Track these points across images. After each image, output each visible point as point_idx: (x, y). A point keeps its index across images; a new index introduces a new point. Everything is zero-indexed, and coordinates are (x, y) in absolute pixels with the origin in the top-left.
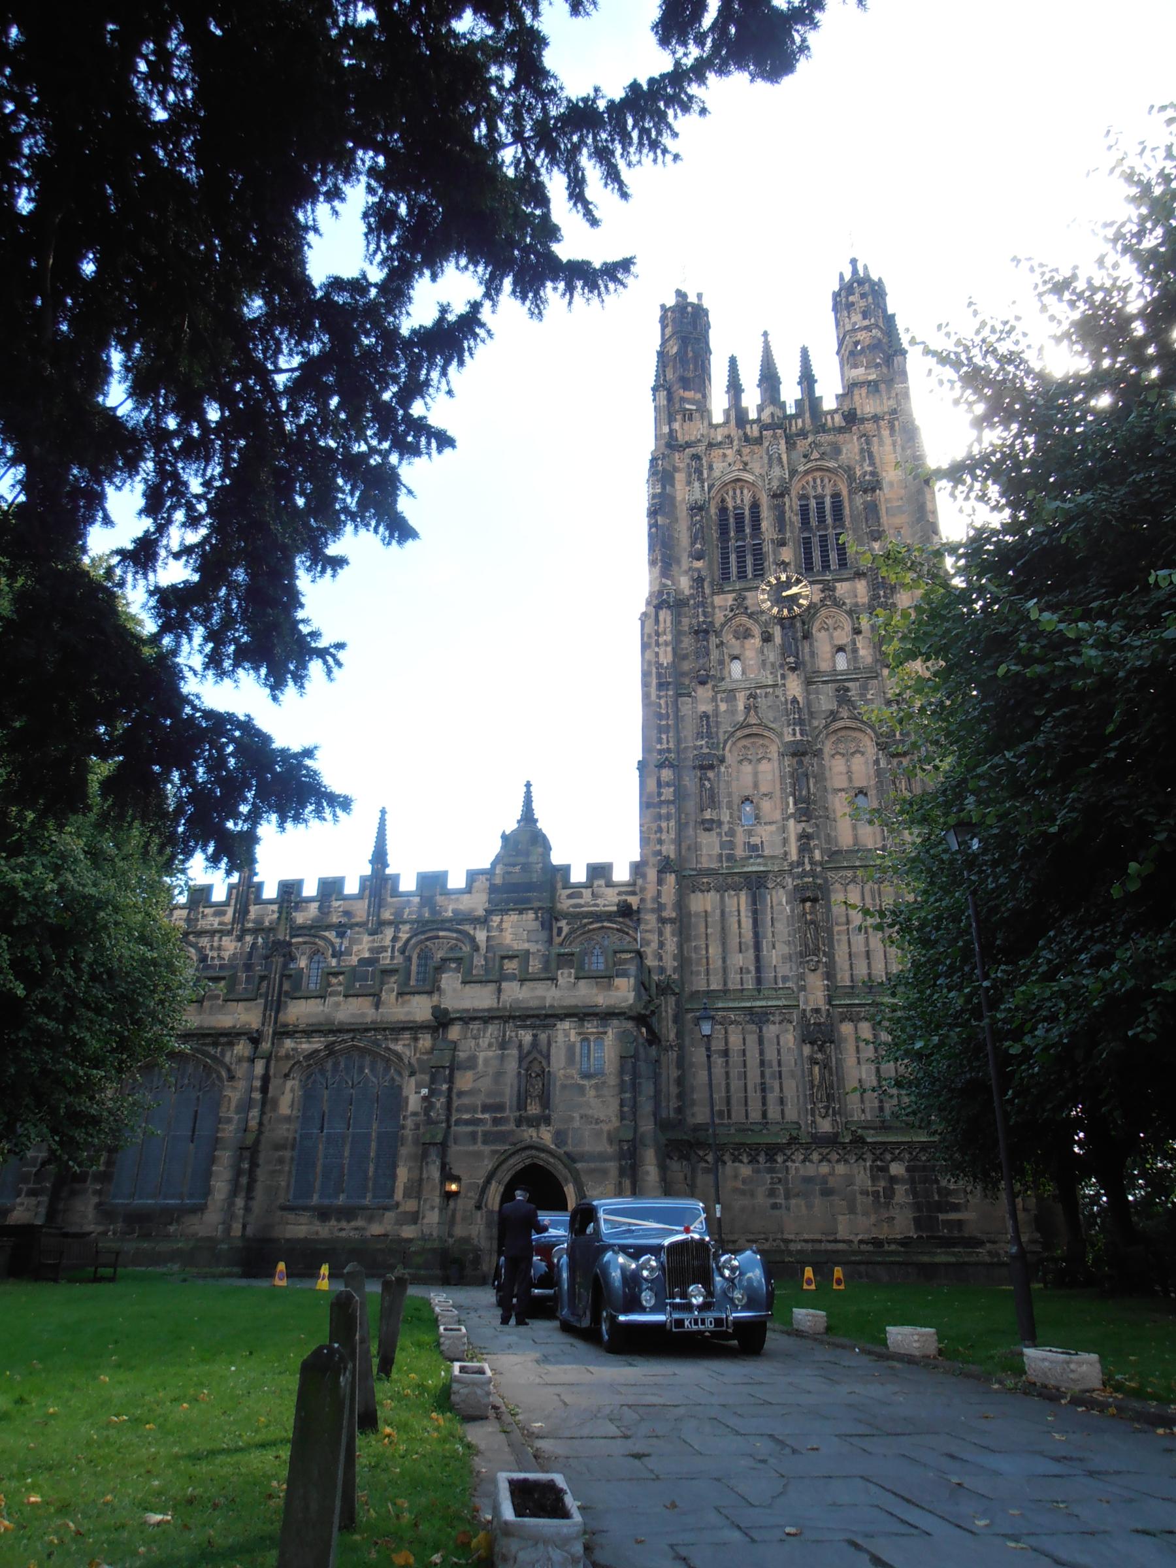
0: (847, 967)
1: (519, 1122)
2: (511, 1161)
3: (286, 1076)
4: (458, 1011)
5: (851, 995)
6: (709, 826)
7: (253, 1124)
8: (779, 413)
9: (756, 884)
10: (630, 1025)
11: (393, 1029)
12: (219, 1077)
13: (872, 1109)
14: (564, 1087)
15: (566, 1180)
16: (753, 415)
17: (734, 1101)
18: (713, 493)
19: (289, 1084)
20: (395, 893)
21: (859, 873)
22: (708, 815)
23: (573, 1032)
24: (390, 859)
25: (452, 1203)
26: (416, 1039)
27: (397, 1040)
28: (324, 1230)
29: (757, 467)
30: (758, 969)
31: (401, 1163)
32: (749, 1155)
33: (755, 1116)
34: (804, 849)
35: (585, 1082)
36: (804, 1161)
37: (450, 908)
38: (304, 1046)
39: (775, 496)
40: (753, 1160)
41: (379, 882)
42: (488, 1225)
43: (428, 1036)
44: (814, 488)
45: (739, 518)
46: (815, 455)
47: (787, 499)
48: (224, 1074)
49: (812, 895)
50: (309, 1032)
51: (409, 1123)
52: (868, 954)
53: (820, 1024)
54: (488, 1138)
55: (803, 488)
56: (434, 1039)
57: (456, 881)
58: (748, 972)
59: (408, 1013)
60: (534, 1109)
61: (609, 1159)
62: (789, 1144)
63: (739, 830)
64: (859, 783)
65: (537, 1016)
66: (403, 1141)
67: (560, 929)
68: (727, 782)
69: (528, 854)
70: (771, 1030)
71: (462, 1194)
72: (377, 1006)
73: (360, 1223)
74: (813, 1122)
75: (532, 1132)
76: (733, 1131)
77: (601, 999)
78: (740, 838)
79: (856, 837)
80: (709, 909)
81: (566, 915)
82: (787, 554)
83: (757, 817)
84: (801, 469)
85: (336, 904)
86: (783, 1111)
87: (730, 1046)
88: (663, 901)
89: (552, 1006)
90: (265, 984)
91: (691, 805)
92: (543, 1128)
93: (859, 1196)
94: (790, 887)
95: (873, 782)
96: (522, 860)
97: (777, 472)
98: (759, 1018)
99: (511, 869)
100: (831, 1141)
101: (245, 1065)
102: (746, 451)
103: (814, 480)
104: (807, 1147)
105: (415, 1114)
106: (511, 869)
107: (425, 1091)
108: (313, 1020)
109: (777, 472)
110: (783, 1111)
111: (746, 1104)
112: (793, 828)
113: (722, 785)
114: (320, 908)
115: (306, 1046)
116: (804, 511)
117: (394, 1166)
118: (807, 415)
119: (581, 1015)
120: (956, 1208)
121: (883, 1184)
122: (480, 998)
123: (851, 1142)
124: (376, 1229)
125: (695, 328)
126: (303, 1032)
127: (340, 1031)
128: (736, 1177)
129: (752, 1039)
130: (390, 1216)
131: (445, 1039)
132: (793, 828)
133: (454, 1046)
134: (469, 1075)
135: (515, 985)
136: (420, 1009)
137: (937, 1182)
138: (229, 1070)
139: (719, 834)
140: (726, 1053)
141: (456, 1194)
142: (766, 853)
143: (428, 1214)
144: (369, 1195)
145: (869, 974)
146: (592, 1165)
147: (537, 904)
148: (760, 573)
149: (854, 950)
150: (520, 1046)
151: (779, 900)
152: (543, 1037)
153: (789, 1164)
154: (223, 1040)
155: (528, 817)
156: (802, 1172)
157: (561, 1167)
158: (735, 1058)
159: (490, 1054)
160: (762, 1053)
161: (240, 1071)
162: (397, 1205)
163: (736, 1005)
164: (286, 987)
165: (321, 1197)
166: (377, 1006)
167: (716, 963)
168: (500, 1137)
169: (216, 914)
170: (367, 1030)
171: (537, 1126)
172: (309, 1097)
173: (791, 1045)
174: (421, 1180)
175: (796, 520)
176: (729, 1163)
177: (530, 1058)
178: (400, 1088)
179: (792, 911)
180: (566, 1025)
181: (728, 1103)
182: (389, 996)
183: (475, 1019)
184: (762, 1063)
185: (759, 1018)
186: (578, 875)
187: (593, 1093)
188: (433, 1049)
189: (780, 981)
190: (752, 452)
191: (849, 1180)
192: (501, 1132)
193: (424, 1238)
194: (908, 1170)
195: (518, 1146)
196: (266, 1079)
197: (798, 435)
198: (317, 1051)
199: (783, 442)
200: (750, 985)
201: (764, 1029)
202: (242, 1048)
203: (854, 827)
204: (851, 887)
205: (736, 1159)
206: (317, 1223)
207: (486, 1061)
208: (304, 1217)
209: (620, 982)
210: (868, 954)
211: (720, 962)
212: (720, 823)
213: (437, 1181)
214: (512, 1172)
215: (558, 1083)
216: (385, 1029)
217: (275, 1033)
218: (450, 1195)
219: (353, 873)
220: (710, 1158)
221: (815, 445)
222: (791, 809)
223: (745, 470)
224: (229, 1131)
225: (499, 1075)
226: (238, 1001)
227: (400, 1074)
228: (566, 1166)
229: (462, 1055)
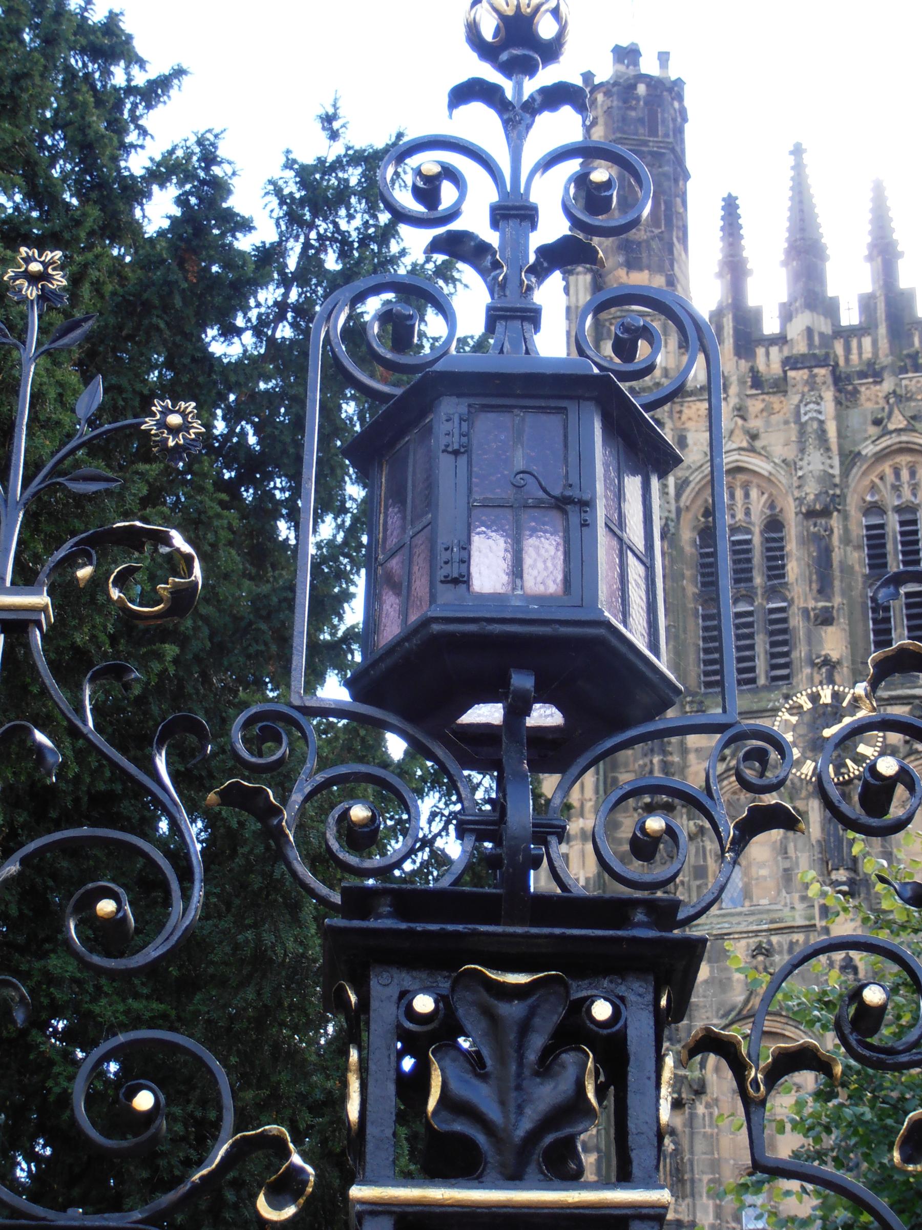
8: (824, 326)
16: (771, 326)
18: (685, 499)
29: (779, 442)
39: (811, 514)
44: (896, 488)
45: (742, 551)
46: (898, 421)
47: (835, 521)
55: (873, 488)
68: (708, 1137)
82: (834, 642)
84: (869, 449)
97: (815, 462)
102: (755, 406)
103: (897, 473)
109: (815, 462)
113: (700, 1146)
116: (876, 541)
118: (882, 330)
125: (653, 132)
148: (782, 674)
175: (857, 559)
190: (768, 410)
197: (862, 375)
199: (829, 395)
221: (899, 398)
223: (752, 450)
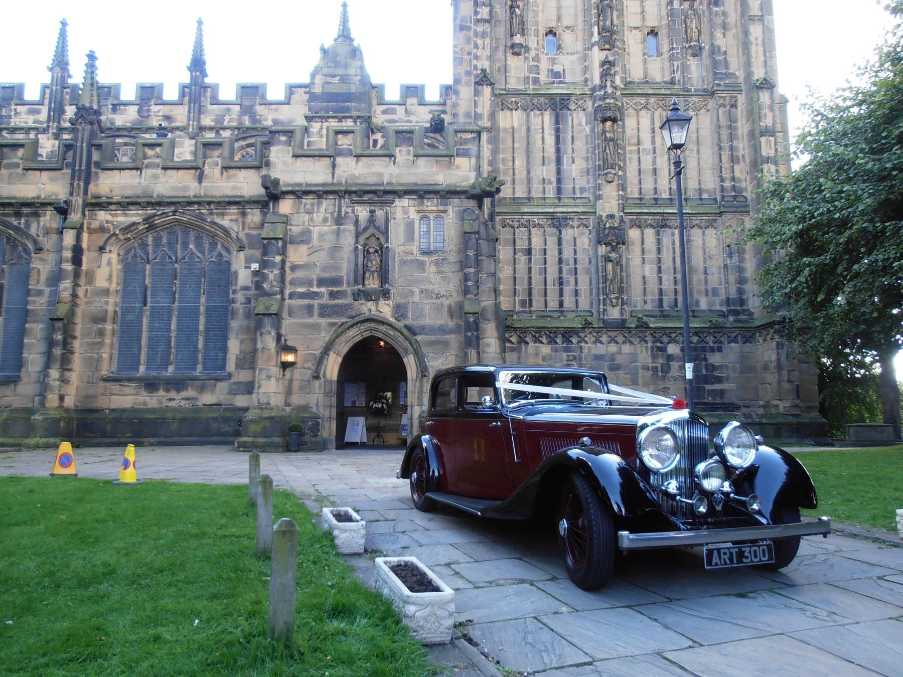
0: (636, 182)
2: (351, 333)
3: (102, 249)
4: (289, 185)
5: (639, 205)
6: (517, 50)
7: (66, 295)
9: (559, 105)
10: (472, 203)
11: (219, 203)
12: (26, 250)
13: (653, 301)
14: (404, 263)
15: (406, 352)
17: (534, 292)
19: (105, 257)
20: (215, 102)
21: (652, 100)
22: (518, 39)
23: (412, 209)
24: (208, 68)
25: (288, 372)
26: (244, 214)
27: (223, 215)
28: (153, 400)
30: (559, 181)
33: (553, 304)
34: (604, 75)
35: (425, 258)
36: (595, 342)
37: (270, 118)
38: (121, 219)
40: (552, 341)
41: (197, 92)
42: (327, 394)
43: (257, 212)
48: (30, 246)
49: (608, 116)
50: (125, 205)
51: (240, 297)
52: (655, 171)
53: (614, 228)
54: (324, 311)
56: (264, 214)
57: (276, 93)
58: (550, 183)
59: (234, 188)
60: (372, 283)
62: (583, 328)
63: (544, 58)
64: (652, 22)
65: (374, 192)
66: (233, 314)
67: (375, 142)
69: (346, 66)
70: (567, 234)
71: (298, 365)
72: (200, 179)
73: (190, 393)
74: (604, 310)
75: (370, 305)
76: (534, 317)
77: (442, 177)
78: (544, 66)
79: (645, 71)
80: (516, 125)
81: (381, 129)
83: (559, 47)
85: (154, 108)
86: (577, 301)
87: (533, 246)
88: (479, 111)
89: (389, 184)
90: (70, 153)
91: (501, 31)
92: (382, 302)
93: (640, 371)
94: (590, 109)
95: (664, 22)
96: (340, 71)
98: (559, 222)
99: (330, 80)
100: (620, 326)
101: (54, 237)
104: (599, 330)
105: (246, 288)
106: (330, 80)
107: (255, 266)
108: (128, 193)
110: (577, 301)
111: (546, 296)
112: (597, 55)
114: (139, 112)
115: (123, 219)
117: (225, 339)
119: (421, 193)
120: (719, 380)
121: (661, 361)
122: (314, 173)
123: (636, 328)
124: (208, 398)
126: (118, 203)
127: (159, 204)
128: (537, 354)
129: (552, 241)
130: (222, 386)
131: (275, 213)
132: (597, 55)
133: (286, 220)
134: (304, 248)
135: (351, 161)
136: (248, 184)
137: (706, 359)
138: (35, 242)
139: (526, 58)
140: (529, 252)
141: (292, 364)
142: (567, 80)
143: (263, 382)
144: (200, 367)
145: (656, 189)
147: (355, 114)
149: (643, 167)
150: (357, 221)
151: (579, 121)
152: (380, 213)
153: (583, 344)
154: (25, 210)
155: (345, 35)
156: (593, 352)
157: (401, 339)
158: (536, 256)
159: (325, 229)
160: (560, 252)
161: (48, 243)
162: (230, 376)
163: (540, 210)
164: (96, 157)
165: (147, 369)
166: (200, 179)
167: (521, 174)
168: (337, 311)
169: (31, 112)
170: (190, 203)
171: (377, 300)
172: (130, 271)
173: (586, 246)
174: (255, 351)
176: (531, 344)
177: (368, 234)
178: (228, 263)
179: (592, 131)
180: (405, 202)
181: (530, 294)
182: (212, 171)
183: (307, 193)
184: (560, 261)
185: (559, 222)
186: (392, 94)
187: (433, 269)
188: (262, 226)
189: (577, 192)
191: (634, 357)
192: (336, 305)
193: (260, 407)
194: (682, 350)
195: (357, 319)
196: (77, 251)
198: (134, 224)
200: (551, 193)
201: (563, 232)
202: (49, 219)
203: (645, 63)
204: (643, 112)
205: (537, 340)
206: (145, 394)
207: (321, 235)
208: (130, 388)
209: (459, 161)
210: (655, 171)
211: (525, 173)
212: (527, 49)
213: (273, 350)
214: (350, 344)
215: (397, 259)
216: (209, 203)
217: (86, 205)
218: (285, 366)
219: (173, 80)
220: (514, 339)
222: (596, 38)
224: (39, 304)
225: (336, 248)
226: (41, 170)
227: (228, 250)
228: (406, 338)
229: (295, 230)
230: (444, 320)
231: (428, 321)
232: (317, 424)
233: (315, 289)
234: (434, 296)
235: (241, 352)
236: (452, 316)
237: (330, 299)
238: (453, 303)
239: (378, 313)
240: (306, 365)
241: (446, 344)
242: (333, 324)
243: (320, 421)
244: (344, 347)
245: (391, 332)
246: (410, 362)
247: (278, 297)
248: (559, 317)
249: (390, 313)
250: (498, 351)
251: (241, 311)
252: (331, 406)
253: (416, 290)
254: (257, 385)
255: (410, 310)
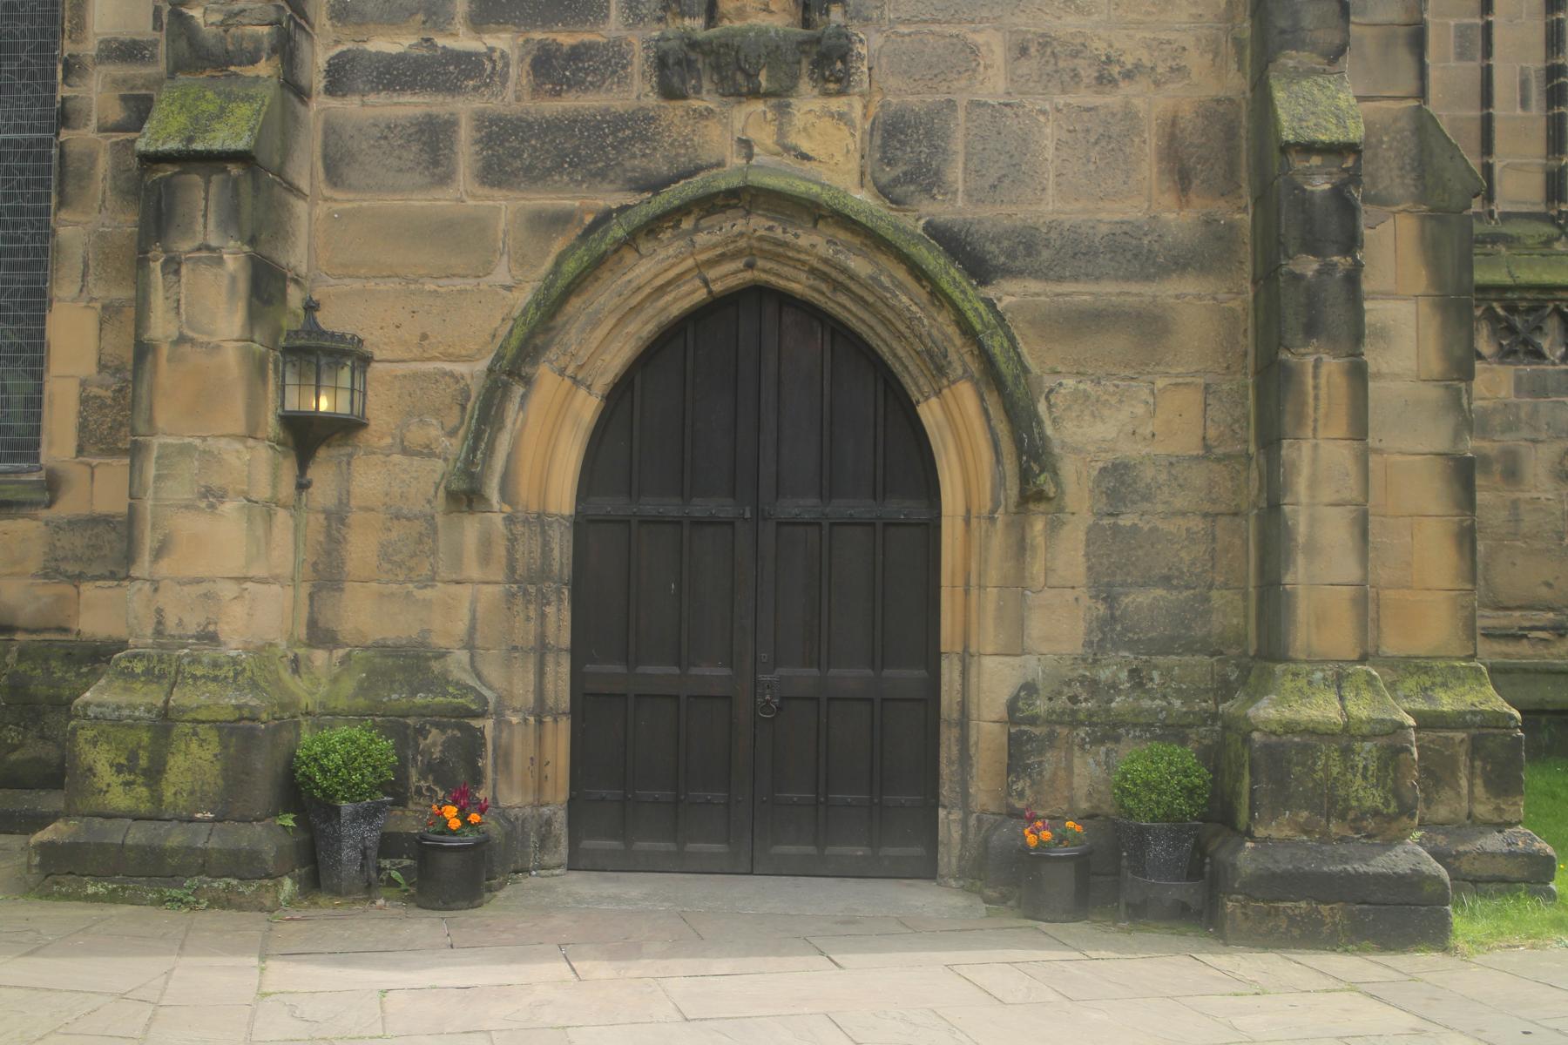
1: (674, 72)
2: (645, 268)
15: (938, 367)
25: (322, 474)
31: (64, 290)
32: (1504, 328)
42: (525, 583)
51: (96, 94)
54: (509, 153)
61: (1180, 262)
75: (751, 118)
92: (808, 104)
105: (127, 51)
117: (36, 302)
141: (344, 429)
146: (1081, 293)
157: (908, 298)
171: (780, 95)
174: (143, 350)
213: (231, 356)
214: (642, 329)
218: (307, 437)
228: (938, 296)
230: (1142, 200)
231: (1053, 202)
232: (472, 745)
233: (464, 41)
234: (1088, 73)
235: (102, 367)
236: (1182, 177)
237: (536, 91)
238: (1187, 112)
239: (789, 160)
240: (416, 436)
241: (1150, 328)
242: (559, 220)
243: (488, 725)
244: (605, 340)
245: (859, 265)
246: (956, 423)
247: (265, 68)
248: (1548, 242)
249: (854, 164)
250: (1435, 365)
251: (103, 164)
252: (542, 649)
253: (993, 44)
254: (148, 541)
255: (958, 145)
